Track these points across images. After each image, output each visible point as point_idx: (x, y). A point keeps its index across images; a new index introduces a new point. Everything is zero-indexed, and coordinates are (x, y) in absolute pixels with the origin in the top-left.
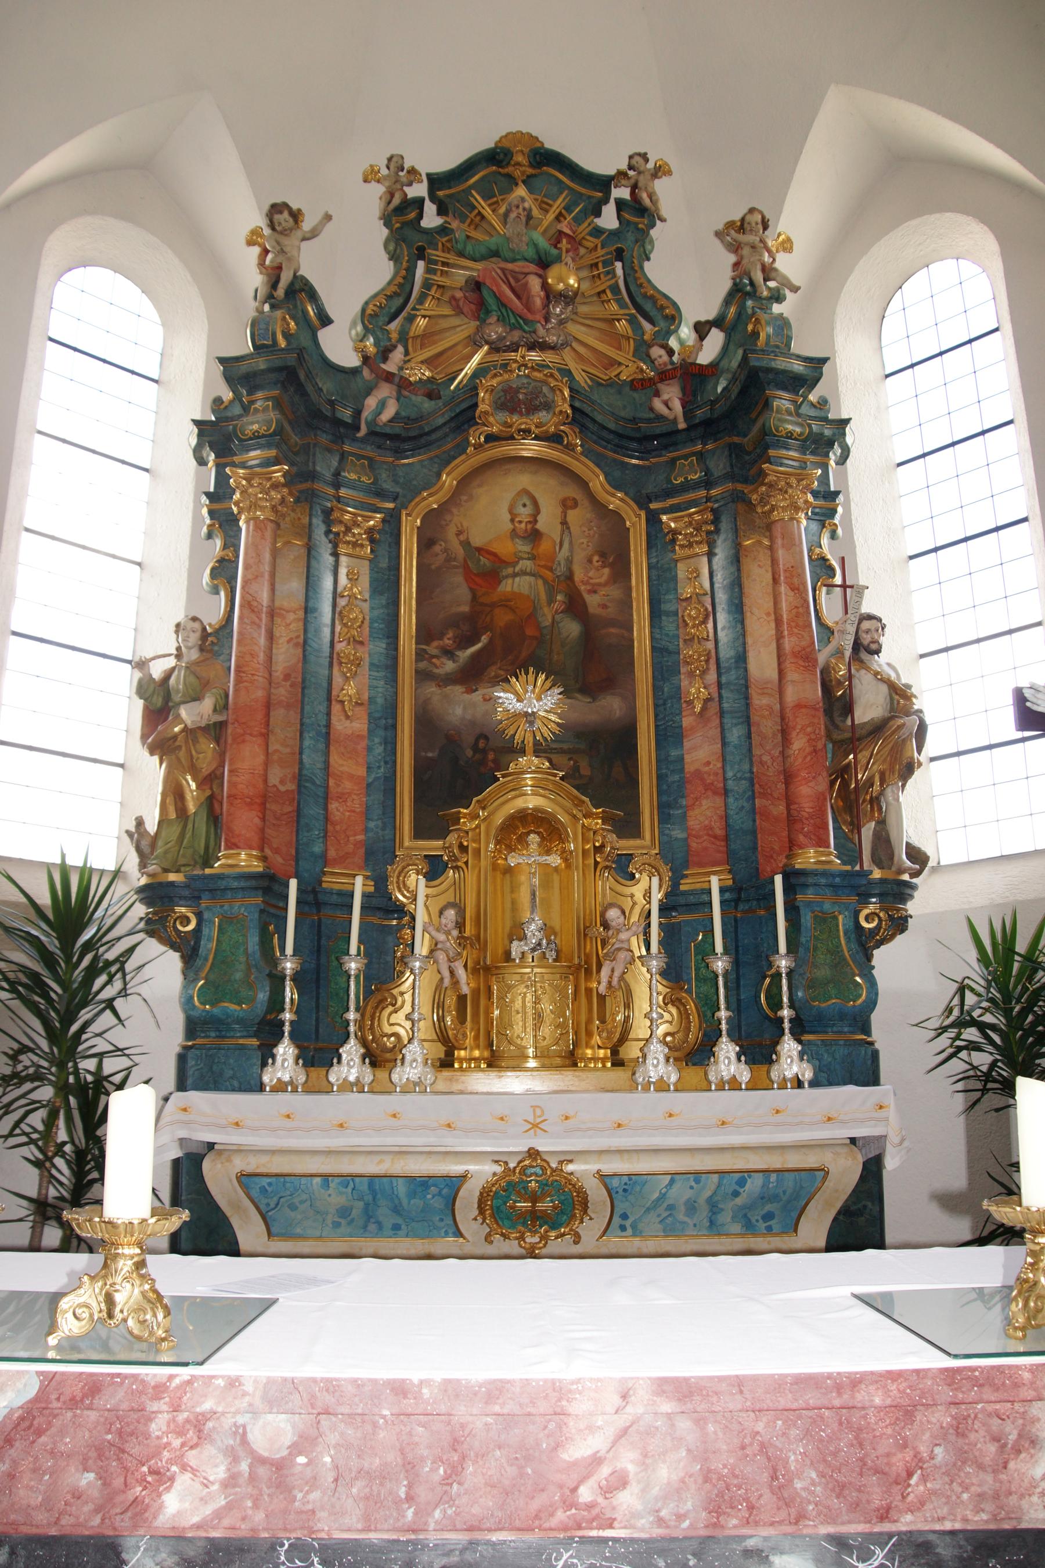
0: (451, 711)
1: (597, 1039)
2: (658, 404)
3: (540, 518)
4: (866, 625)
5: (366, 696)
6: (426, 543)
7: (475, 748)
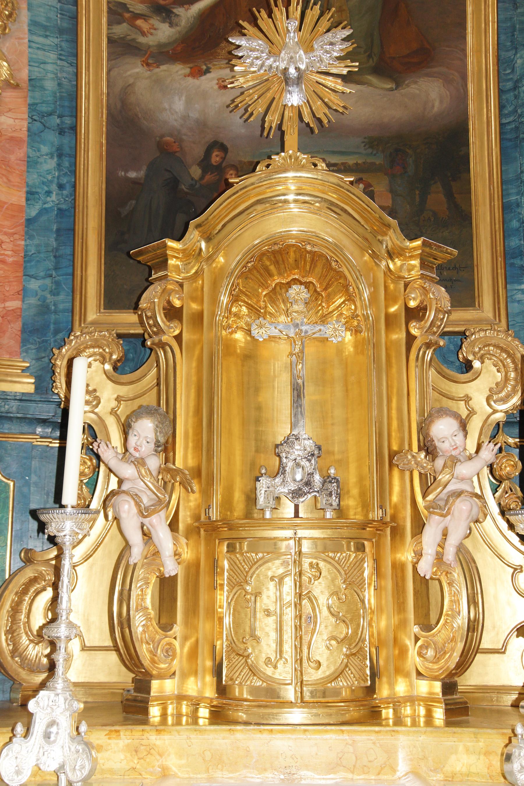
0: (166, 106)
5: (24, 74)
7: (205, 163)
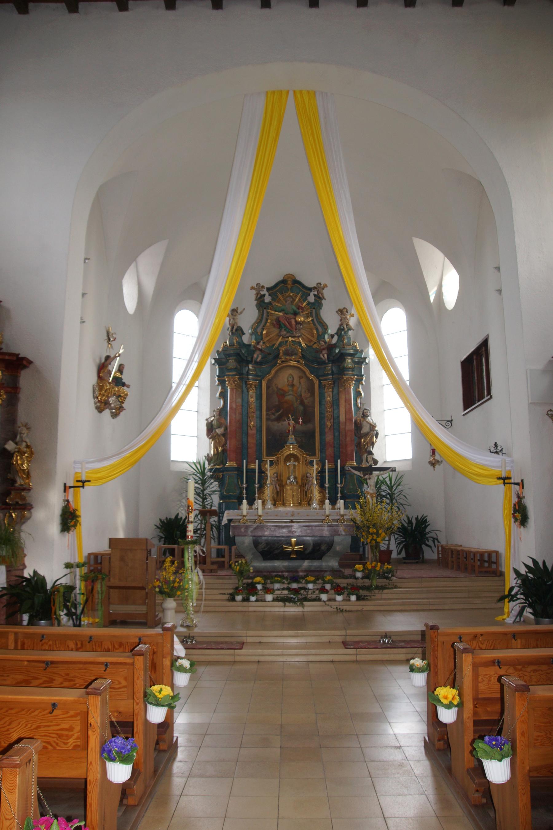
1: (305, 500)
2: (321, 356)
4: (365, 411)
6: (268, 387)
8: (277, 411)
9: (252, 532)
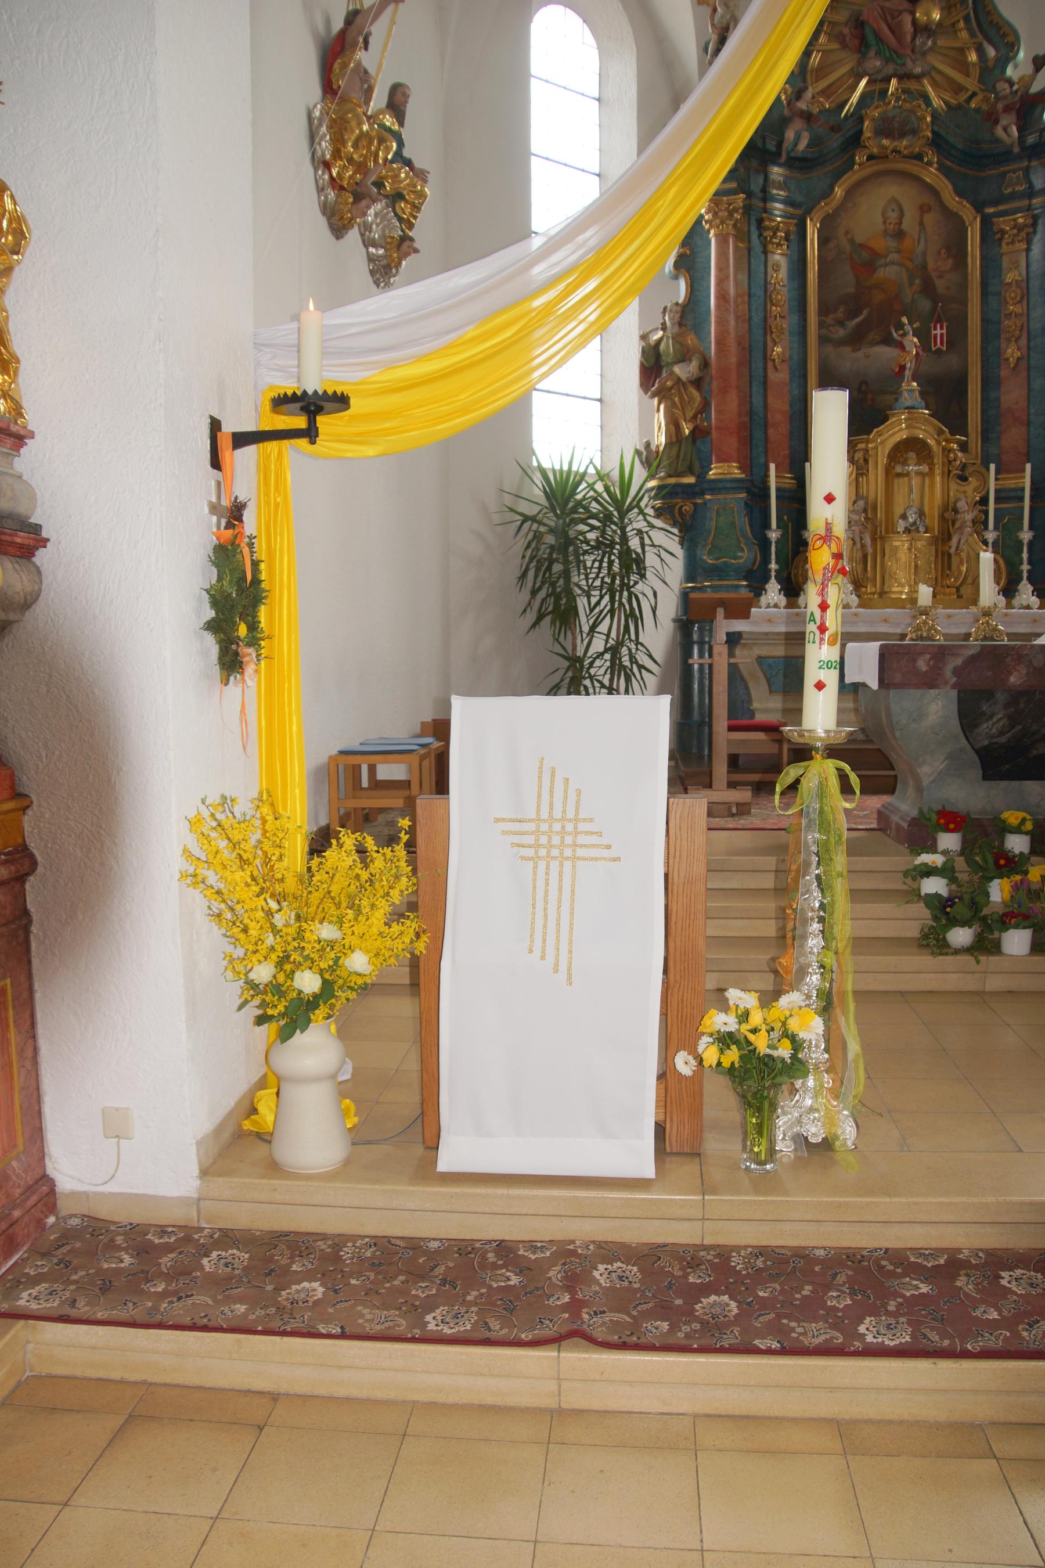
3: (904, 221)
5: (787, 355)
6: (823, 241)
8: (853, 314)
9: (956, 671)
